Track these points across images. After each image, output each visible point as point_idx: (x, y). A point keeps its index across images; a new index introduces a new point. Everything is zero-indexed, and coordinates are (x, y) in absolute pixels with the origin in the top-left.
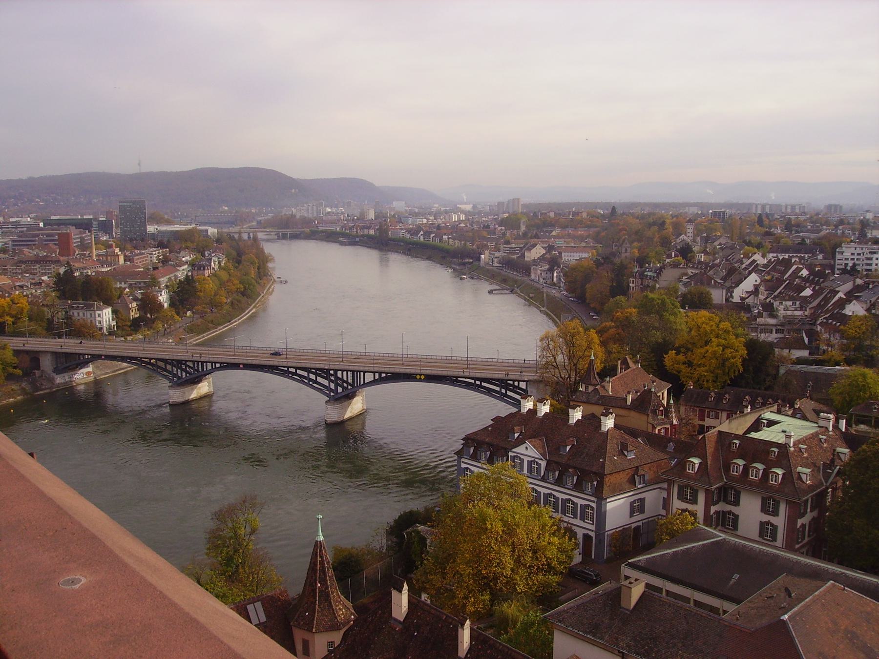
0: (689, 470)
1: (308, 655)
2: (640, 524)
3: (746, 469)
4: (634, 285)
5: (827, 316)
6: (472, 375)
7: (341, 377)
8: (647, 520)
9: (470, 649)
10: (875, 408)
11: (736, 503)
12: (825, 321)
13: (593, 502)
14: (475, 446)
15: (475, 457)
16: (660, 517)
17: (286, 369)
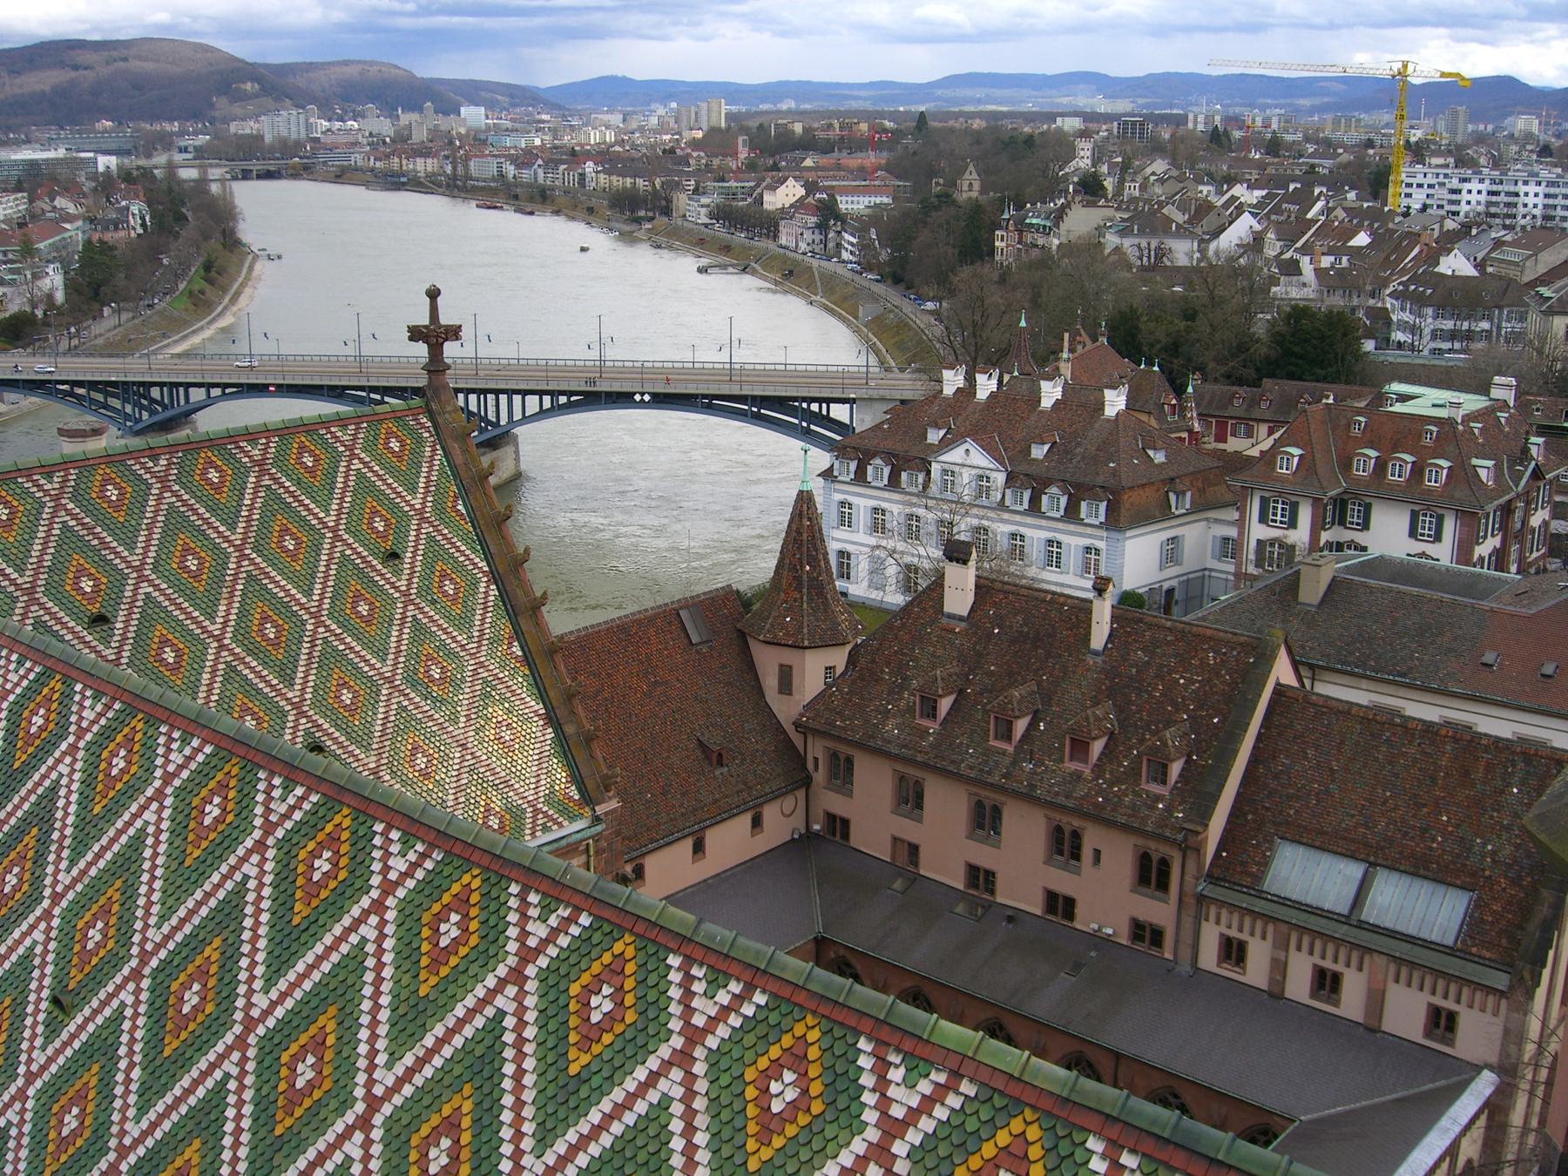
0: (1281, 468)
1: (790, 694)
2: (1174, 583)
3: (1381, 466)
4: (1004, 244)
5: (1405, 279)
6: (747, 391)
7: (475, 410)
8: (1185, 578)
9: (1110, 635)
10: (1538, 410)
11: (1365, 526)
12: (1401, 287)
13: (1101, 539)
14: (859, 459)
15: (860, 478)
16: (1207, 573)
17: (364, 394)
